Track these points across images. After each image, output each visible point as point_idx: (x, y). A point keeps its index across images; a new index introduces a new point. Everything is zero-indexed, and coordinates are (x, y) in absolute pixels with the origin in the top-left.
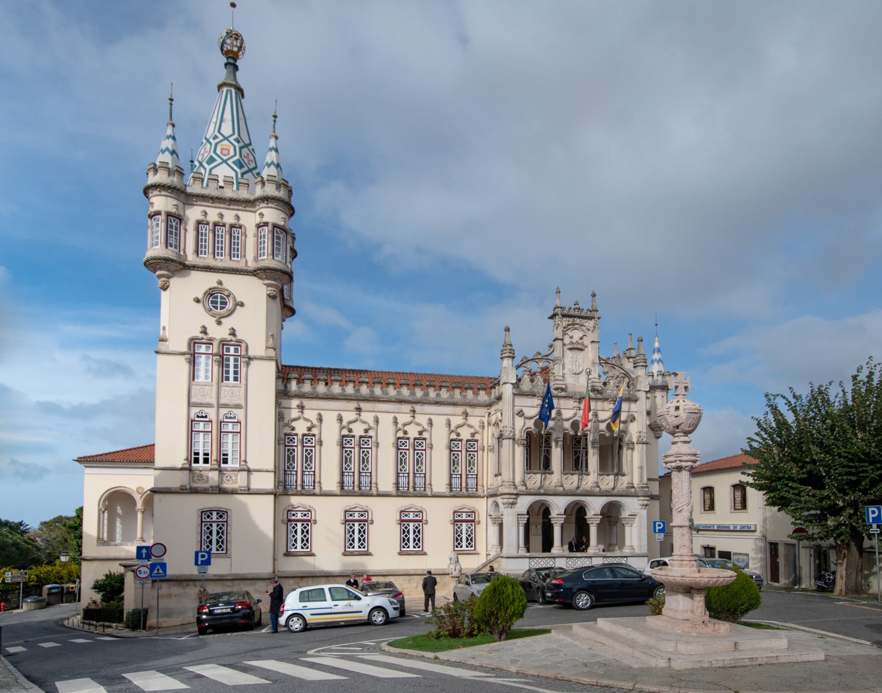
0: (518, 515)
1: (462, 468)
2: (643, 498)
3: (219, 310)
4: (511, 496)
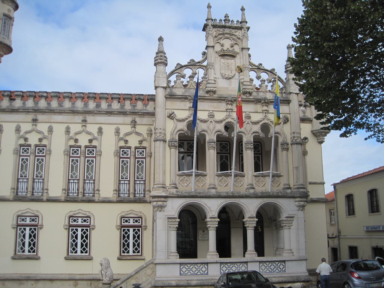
0: (169, 218)
1: (130, 174)
2: (299, 199)
4: (159, 199)
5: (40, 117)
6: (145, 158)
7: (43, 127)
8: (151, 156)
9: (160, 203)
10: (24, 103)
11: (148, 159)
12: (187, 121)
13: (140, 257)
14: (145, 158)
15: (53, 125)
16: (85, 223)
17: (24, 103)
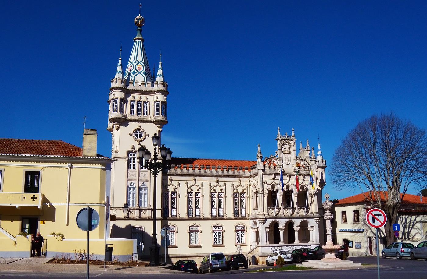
0: (266, 227)
3: (139, 138)
4: (263, 219)
5: (197, 178)
6: (245, 198)
7: (199, 183)
8: (248, 197)
9: (263, 221)
10: (188, 171)
11: (246, 198)
12: (271, 184)
13: (245, 245)
14: (245, 198)
15: (204, 183)
16: (220, 229)
17: (188, 171)
